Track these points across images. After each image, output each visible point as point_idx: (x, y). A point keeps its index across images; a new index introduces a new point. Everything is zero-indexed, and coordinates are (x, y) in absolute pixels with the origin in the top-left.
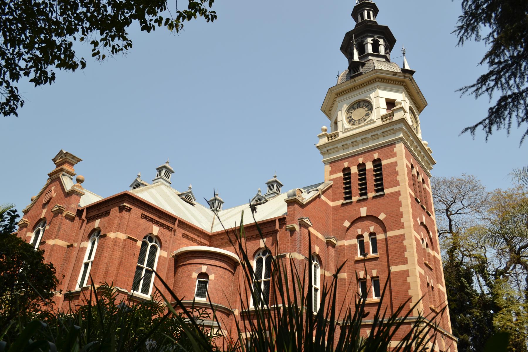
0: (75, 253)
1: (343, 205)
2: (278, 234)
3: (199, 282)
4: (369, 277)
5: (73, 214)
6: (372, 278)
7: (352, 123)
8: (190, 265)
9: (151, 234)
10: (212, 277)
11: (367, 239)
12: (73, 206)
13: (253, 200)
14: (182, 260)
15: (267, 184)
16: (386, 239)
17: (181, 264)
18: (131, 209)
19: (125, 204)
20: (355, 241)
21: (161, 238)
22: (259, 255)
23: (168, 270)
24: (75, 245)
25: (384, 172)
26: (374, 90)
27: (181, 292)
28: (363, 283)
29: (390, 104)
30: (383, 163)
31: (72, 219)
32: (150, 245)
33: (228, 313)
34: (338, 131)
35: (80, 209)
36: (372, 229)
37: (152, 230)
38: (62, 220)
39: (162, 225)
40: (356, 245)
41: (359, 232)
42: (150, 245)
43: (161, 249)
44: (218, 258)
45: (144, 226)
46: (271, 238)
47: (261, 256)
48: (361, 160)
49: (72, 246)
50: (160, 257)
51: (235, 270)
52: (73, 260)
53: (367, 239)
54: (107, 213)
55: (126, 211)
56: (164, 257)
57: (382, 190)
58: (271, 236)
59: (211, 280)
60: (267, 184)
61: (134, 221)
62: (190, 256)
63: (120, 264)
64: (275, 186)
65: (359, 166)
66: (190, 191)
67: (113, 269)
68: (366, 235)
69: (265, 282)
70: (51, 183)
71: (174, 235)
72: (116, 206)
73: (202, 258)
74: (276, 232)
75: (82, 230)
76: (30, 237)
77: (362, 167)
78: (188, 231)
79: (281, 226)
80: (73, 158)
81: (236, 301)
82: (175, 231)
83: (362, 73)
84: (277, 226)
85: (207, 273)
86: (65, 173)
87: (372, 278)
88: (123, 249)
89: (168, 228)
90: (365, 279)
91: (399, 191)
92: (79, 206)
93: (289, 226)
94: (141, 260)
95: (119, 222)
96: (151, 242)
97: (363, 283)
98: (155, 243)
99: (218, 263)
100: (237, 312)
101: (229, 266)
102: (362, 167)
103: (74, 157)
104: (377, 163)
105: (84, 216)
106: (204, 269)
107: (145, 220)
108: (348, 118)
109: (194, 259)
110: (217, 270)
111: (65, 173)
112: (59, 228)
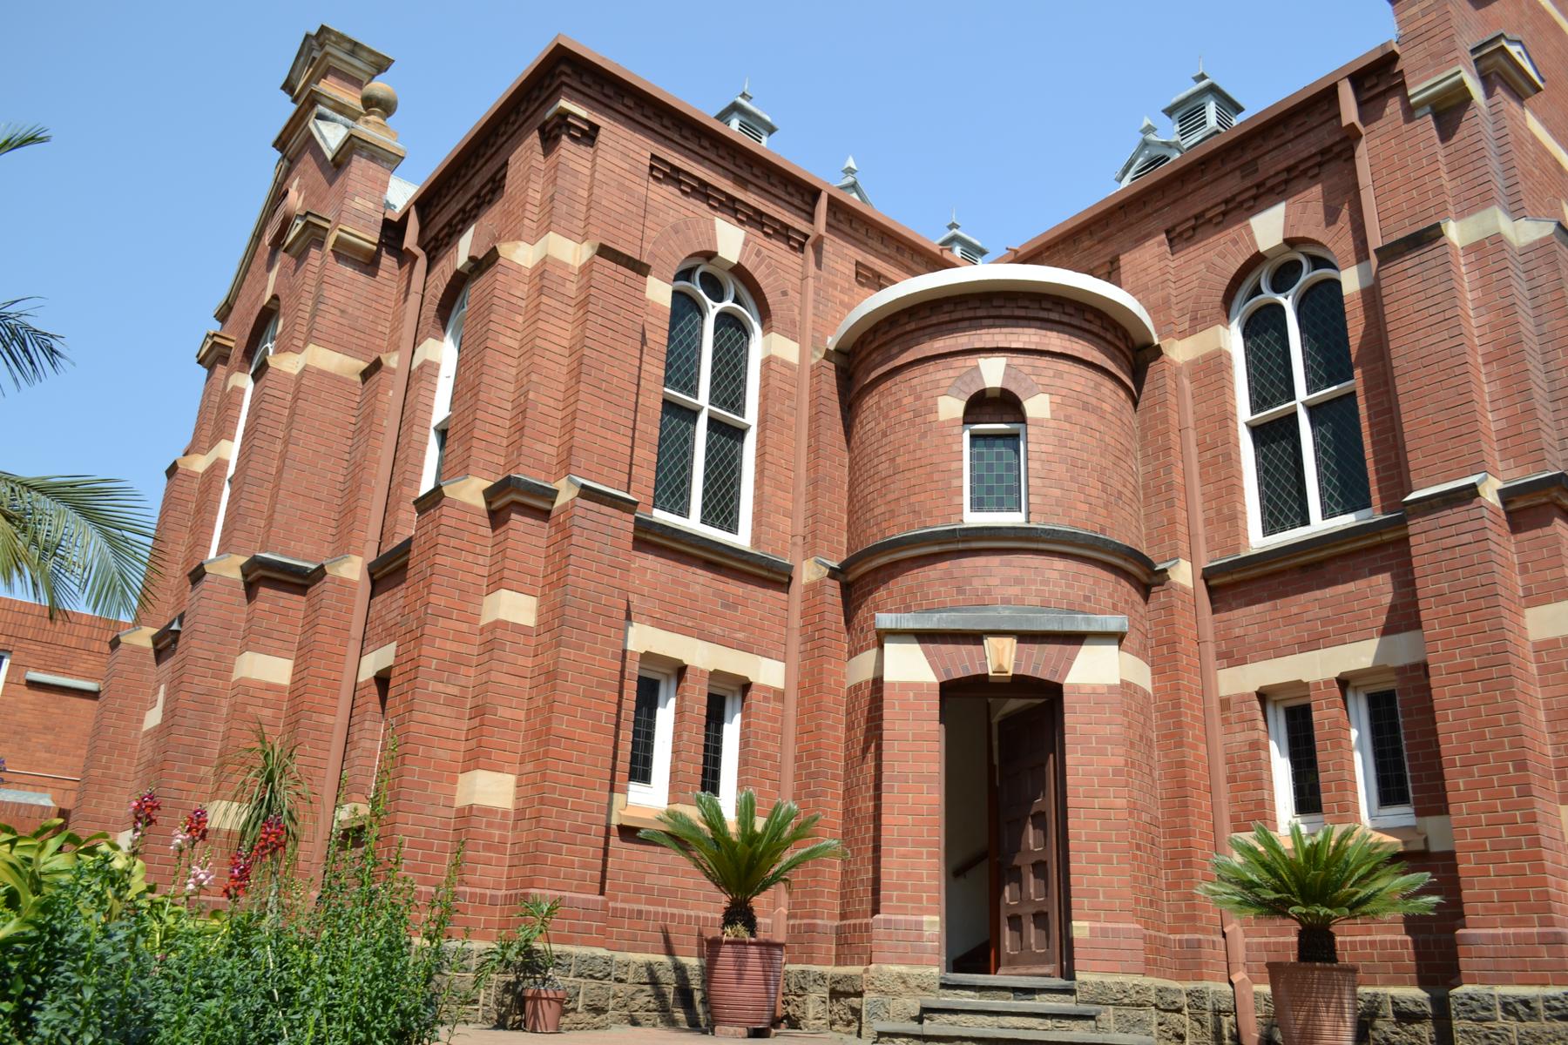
0: (392, 397)
2: (1362, 151)
3: (975, 437)
5: (369, 237)
8: (916, 371)
9: (710, 256)
10: (1036, 407)
12: (359, 203)
13: (1125, 172)
14: (877, 357)
15: (1169, 112)
17: (874, 375)
18: (595, 128)
19: (564, 103)
21: (758, 276)
22: (1257, 291)
23: (814, 420)
24: (392, 361)
27: (890, 497)
31: (369, 264)
32: (713, 309)
33: (1144, 576)
35: (395, 216)
37: (713, 239)
38: (323, 266)
39: (755, 219)
42: (713, 309)
43: (767, 326)
44: (1054, 316)
45: (672, 218)
46: (1317, 190)
47: (1268, 295)
49: (377, 365)
50: (767, 363)
51: (1139, 388)
52: (390, 424)
54: (496, 186)
55: (573, 138)
56: (785, 364)
58: (1314, 179)
59: (1039, 423)
60: (1169, 112)
61: (622, 187)
62: (912, 326)
63: (576, 374)
64: (1211, 110)
66: (850, 180)
67: (547, 400)
69: (1312, 410)
70: (288, 173)
71: (818, 264)
72: (529, 132)
73: (975, 323)
74: (1351, 137)
75: (414, 299)
76: (242, 391)
78: (878, 254)
79: (1370, 107)
80: (352, 53)
81: (1172, 522)
82: (818, 248)
84: (1349, 111)
85: (1012, 387)
86: (328, 112)
88: (583, 304)
89: (783, 232)
92: (388, 205)
93: (1419, 88)
94: (681, 371)
95: (551, 190)
96: (719, 298)
98: (737, 300)
99: (1055, 341)
100: (1183, 574)
101: (1113, 359)
103: (355, 48)
105: (411, 240)
106: (993, 373)
107: (669, 191)
109: (932, 337)
110: (1059, 374)
111: (328, 112)
112: (318, 300)
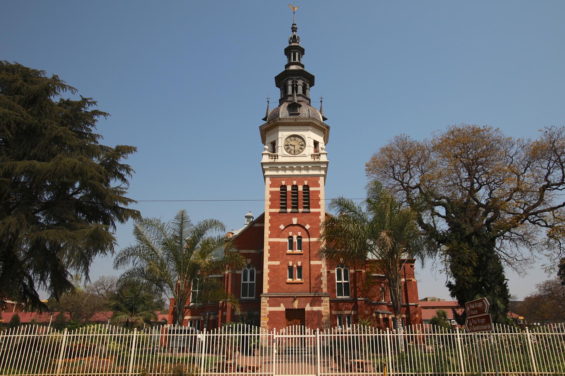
1: (280, 212)
4: (295, 266)
6: (298, 266)
7: (289, 151)
11: (295, 240)
16: (310, 242)
20: (287, 240)
25: (310, 197)
26: (308, 130)
28: (291, 269)
29: (316, 144)
30: (311, 189)
34: (279, 154)
36: (299, 234)
40: (287, 243)
41: (291, 234)
48: (295, 183)
53: (295, 240)
57: (309, 208)
65: (293, 186)
68: (295, 237)
77: (295, 187)
83: (299, 114)
87: (298, 266)
90: (292, 266)
91: (320, 212)
97: (291, 269)
102: (295, 187)
104: (306, 188)
108: (286, 145)
